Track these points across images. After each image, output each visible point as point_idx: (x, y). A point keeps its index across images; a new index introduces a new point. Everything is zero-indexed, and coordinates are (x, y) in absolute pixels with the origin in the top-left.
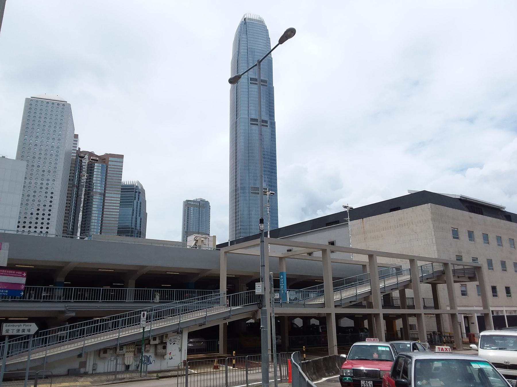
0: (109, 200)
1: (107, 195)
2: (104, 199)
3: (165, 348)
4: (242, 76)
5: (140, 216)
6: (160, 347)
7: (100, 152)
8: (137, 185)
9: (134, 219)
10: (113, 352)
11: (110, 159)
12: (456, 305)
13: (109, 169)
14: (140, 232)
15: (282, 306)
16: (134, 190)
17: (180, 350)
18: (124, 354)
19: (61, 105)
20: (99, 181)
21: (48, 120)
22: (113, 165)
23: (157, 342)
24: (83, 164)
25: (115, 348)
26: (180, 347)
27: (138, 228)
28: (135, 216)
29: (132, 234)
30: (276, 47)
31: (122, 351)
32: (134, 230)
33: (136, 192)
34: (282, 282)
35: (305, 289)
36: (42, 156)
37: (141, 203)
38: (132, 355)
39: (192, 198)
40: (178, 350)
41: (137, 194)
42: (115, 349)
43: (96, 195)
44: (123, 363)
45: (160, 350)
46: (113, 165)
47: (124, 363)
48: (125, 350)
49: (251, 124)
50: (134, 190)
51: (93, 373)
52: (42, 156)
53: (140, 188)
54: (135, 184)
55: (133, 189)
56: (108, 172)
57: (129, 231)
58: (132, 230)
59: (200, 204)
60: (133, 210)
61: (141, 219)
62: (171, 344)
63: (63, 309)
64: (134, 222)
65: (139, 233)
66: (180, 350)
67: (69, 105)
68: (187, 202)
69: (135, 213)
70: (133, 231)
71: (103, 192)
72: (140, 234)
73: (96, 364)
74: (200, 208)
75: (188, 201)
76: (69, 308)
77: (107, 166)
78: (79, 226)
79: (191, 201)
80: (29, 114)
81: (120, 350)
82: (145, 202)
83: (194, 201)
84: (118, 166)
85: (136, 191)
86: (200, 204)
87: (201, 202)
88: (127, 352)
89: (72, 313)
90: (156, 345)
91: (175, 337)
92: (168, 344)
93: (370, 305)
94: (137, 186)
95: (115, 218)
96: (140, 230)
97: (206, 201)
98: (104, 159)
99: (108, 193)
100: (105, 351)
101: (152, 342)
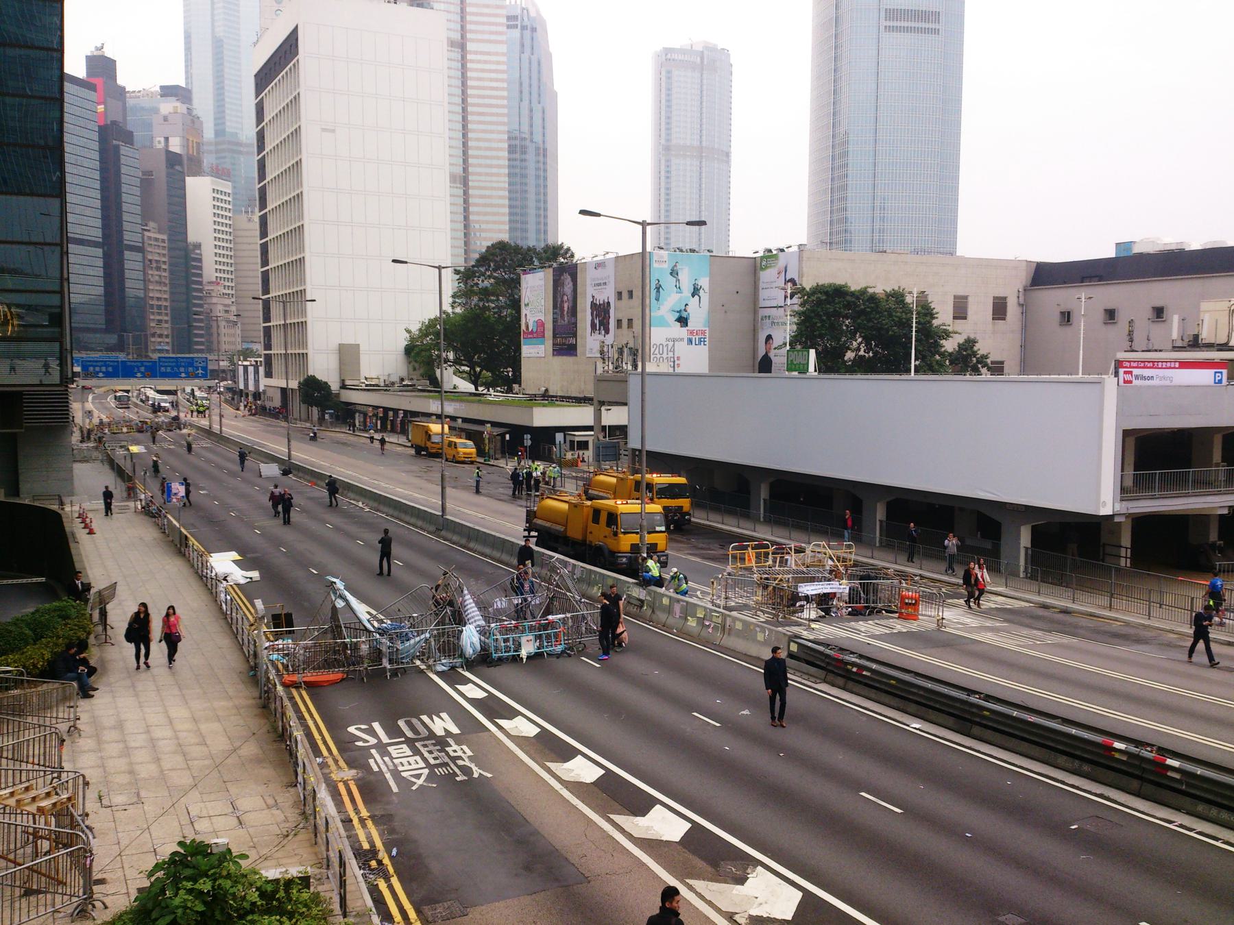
2: (463, 57)
8: (523, 6)
9: (525, 112)
14: (545, 150)
16: (519, 23)
27: (538, 138)
28: (528, 102)
29: (523, 157)
32: (528, 143)
33: (524, 28)
39: (678, 41)
41: (527, 33)
50: (519, 23)
53: (533, 14)
59: (702, 59)
60: (521, 84)
64: (525, 121)
65: (542, 151)
68: (666, 55)
71: (460, 38)
72: (545, 156)
74: (705, 72)
75: (667, 51)
82: (549, 56)
83: (682, 51)
85: (525, 24)
86: (702, 59)
87: (706, 53)
94: (523, 9)
95: (497, 115)
99: (472, 40)
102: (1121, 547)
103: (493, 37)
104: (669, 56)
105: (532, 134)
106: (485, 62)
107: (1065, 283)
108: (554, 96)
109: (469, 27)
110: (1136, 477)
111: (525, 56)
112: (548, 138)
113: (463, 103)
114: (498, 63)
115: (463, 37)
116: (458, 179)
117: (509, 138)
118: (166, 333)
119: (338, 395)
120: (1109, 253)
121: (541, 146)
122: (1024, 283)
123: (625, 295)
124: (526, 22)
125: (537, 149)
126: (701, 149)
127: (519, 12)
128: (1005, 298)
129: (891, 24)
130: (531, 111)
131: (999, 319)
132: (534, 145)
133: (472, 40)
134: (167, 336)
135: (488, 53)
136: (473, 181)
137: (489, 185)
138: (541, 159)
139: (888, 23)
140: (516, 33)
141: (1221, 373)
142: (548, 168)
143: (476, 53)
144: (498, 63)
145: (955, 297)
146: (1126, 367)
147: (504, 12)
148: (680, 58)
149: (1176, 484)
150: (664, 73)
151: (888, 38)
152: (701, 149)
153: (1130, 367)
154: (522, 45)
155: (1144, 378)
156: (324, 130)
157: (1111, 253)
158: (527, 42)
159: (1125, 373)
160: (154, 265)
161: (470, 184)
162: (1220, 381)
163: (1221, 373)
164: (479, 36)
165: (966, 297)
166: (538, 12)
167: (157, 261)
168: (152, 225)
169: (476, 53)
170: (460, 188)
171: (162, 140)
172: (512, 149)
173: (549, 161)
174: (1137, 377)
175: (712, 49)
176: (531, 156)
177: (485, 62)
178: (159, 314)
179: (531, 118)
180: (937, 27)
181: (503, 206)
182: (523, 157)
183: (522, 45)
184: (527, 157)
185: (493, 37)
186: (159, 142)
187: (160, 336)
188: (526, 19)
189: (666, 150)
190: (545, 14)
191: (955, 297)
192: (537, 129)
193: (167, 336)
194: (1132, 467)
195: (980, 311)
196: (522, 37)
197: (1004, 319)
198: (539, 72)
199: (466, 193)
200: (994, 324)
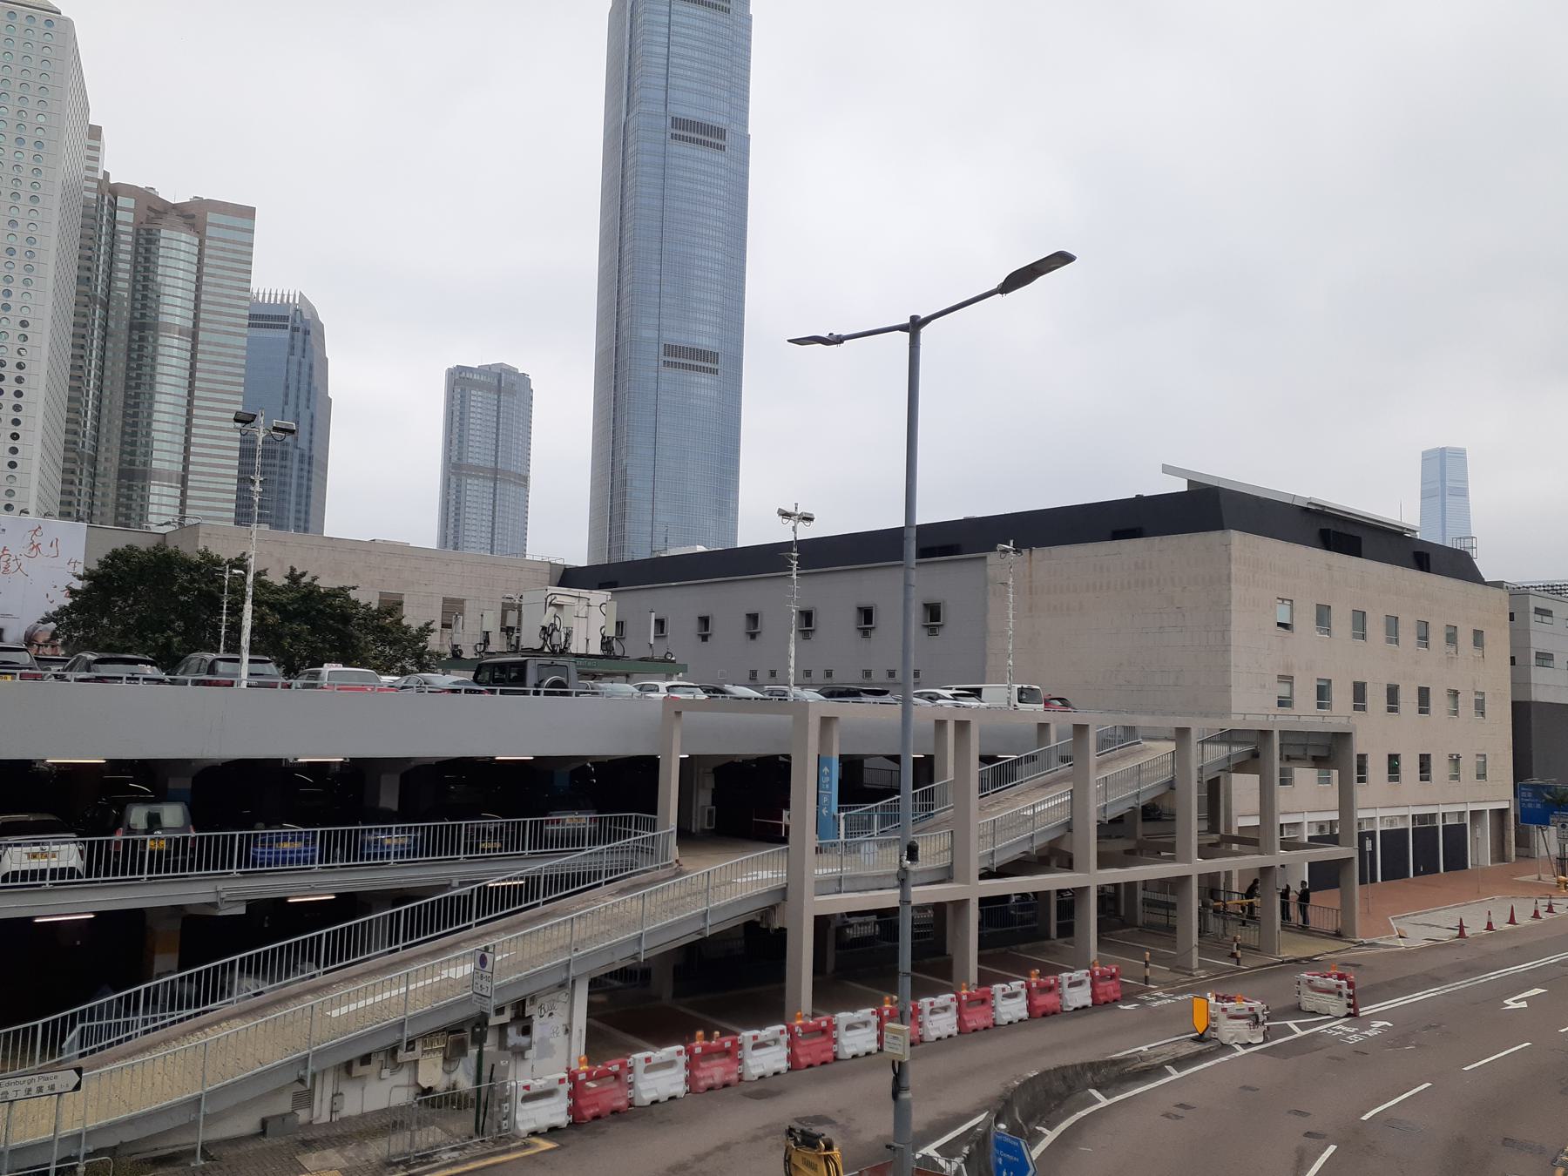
0: (212, 353)
1: (202, 336)
2: (194, 347)
3: (527, 1031)
4: (845, 342)
6: (512, 1032)
7: (174, 192)
10: (386, 1056)
12: (1276, 811)
14: (310, 458)
15: (843, 888)
17: (567, 1030)
18: (416, 1062)
19: (40, 22)
22: (219, 239)
23: (506, 1018)
25: (393, 1051)
26: (565, 1020)
29: (284, 463)
30: (985, 298)
31: (410, 1053)
32: (290, 449)
33: (295, 329)
34: (827, 786)
35: (891, 802)
37: (311, 368)
38: (439, 1058)
40: (561, 1031)
41: (299, 335)
42: (393, 1051)
43: (168, 334)
44: (412, 1082)
45: (513, 1037)
46: (219, 239)
47: (418, 1084)
48: (419, 1047)
49: (672, 138)
50: (289, 324)
51: (333, 1120)
53: (307, 316)
54: (291, 301)
55: (286, 318)
57: (275, 451)
58: (285, 449)
61: (312, 417)
62: (541, 1017)
65: (306, 459)
66: (568, 1031)
67: (68, 23)
68: (461, 373)
72: (310, 464)
73: (341, 1094)
75: (461, 369)
76: (229, 896)
78: (243, 643)
79: (471, 370)
80: (16, 186)
81: (407, 1050)
84: (234, 242)
85: (296, 325)
86: (499, 381)
88: (424, 1052)
89: (237, 906)
90: (502, 1028)
91: (554, 996)
92: (536, 1019)
93: (1068, 864)
96: (310, 449)
97: (520, 372)
98: (192, 216)
99: (205, 330)
100: (366, 1059)
101: (494, 1020)
103: (232, 329)
106: (220, 354)
109: (202, 315)
111: (295, 359)
112: (315, 446)
113: (189, 395)
114: (235, 356)
115: (195, 325)
116: (174, 476)
121: (306, 453)
125: (302, 456)
126: (496, 471)
132: (298, 451)
133: (205, 330)
135: (224, 346)
136: (192, 481)
137: (212, 486)
138: (306, 467)
139: (667, 359)
140: (285, 335)
142: (314, 477)
143: (209, 343)
144: (235, 356)
145: (445, 600)
147: (247, 304)
148: (475, 377)
151: (668, 373)
152: (496, 471)
154: (293, 347)
158: (299, 344)
161: (190, 483)
164: (215, 327)
165: (462, 601)
169: (209, 343)
170: (177, 488)
175: (511, 372)
177: (220, 354)
180: (716, 368)
181: (229, 510)
182: (284, 463)
183: (293, 347)
184: (289, 464)
185: (232, 329)
188: (298, 320)
189: (456, 469)
191: (445, 600)
196: (292, 338)
198: (310, 376)
199: (183, 493)
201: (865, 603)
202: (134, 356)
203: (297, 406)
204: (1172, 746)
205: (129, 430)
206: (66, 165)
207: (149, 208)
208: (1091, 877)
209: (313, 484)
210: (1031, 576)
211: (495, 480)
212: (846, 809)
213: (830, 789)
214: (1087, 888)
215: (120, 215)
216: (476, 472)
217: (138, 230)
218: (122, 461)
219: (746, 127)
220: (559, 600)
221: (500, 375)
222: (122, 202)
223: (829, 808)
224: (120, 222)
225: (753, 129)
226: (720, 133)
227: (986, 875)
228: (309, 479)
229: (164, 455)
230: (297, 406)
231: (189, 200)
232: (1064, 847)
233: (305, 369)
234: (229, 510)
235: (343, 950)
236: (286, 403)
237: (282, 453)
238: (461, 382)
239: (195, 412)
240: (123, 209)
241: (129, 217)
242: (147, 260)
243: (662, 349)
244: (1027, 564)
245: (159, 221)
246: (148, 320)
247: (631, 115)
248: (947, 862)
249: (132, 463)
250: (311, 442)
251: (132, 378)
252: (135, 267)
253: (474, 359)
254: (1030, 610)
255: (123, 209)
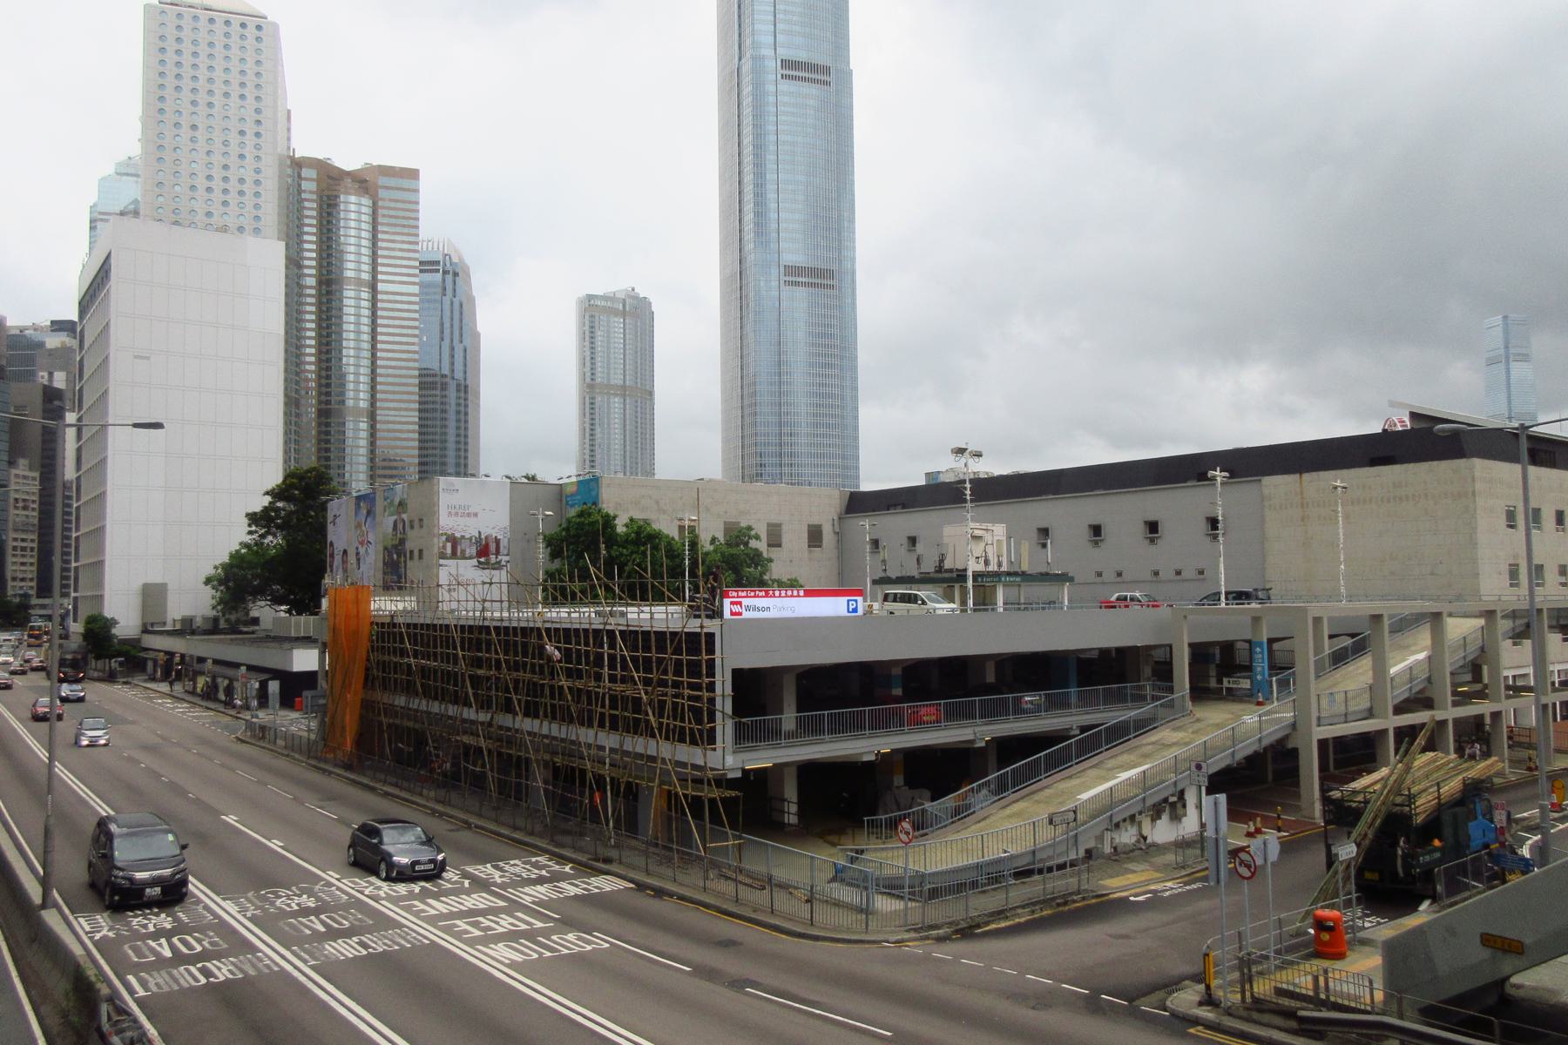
1: (380, 286)
5: (461, 342)
7: (347, 161)
11: (382, 181)
13: (380, 212)
14: (466, 387)
19: (251, 29)
20: (353, 247)
21: (219, 74)
22: (391, 200)
24: (304, 196)
27: (459, 375)
32: (448, 380)
36: (217, 184)
38: (1149, 819)
41: (449, 278)
46: (391, 200)
52: (217, 184)
53: (455, 260)
54: (441, 249)
55: (437, 263)
56: (380, 220)
57: (436, 383)
58: (445, 380)
59: (624, 306)
60: (442, 324)
61: (465, 350)
63: (971, 737)
65: (463, 388)
69: (447, 332)
70: (446, 384)
72: (466, 392)
75: (590, 297)
77: (375, 204)
79: (596, 297)
82: (472, 300)
83: (604, 298)
86: (624, 306)
96: (465, 379)
98: (364, 182)
102: (785, 800)
104: (592, 302)
105: (453, 371)
107: (874, 511)
108: (476, 336)
110: (799, 720)
117: (420, 376)
118: (30, 576)
119: (139, 640)
120: (920, 481)
122: (839, 510)
123: (416, 524)
124: (448, 267)
125: (458, 385)
127: (440, 258)
128: (820, 526)
129: (791, 279)
130: (452, 349)
131: (815, 546)
134: (31, 580)
137: (398, 419)
138: (462, 395)
139: (787, 279)
140: (439, 276)
141: (856, 601)
143: (387, 293)
146: (733, 597)
147: (416, 255)
149: (841, 727)
150: (587, 317)
152: (624, 387)
153: (738, 597)
155: (756, 609)
156: (136, 357)
157: (922, 482)
159: (732, 603)
160: (20, 504)
161: (378, 418)
162: (855, 610)
163: (856, 601)
165: (779, 525)
166: (461, 259)
167: (24, 500)
168: (22, 462)
171: (45, 374)
172: (422, 386)
173: (470, 397)
174: (748, 608)
176: (452, 393)
178: (23, 556)
179: (453, 356)
181: (413, 440)
183: (445, 289)
186: (43, 377)
187: (23, 580)
188: (448, 264)
189: (592, 391)
190: (468, 261)
191: (769, 525)
192: (459, 366)
193: (31, 580)
194: (794, 707)
195: (795, 538)
196: (444, 280)
197: (820, 546)
200: (810, 552)
201: (1151, 518)
202: (324, 309)
203: (452, 340)
204: (1482, 622)
205: (324, 373)
206: (281, 149)
207: (330, 177)
208: (1450, 713)
209: (470, 411)
210: (1302, 493)
211: (624, 396)
212: (1277, 674)
213: (1263, 662)
214: (1447, 720)
215: (305, 185)
216: (609, 389)
217: (321, 197)
218: (320, 402)
219: (848, 63)
220: (977, 533)
221: (624, 300)
222: (306, 172)
223: (1263, 675)
224: (304, 191)
225: (854, 64)
226: (826, 70)
227: (1399, 709)
228: (466, 406)
229: (356, 394)
230: (452, 340)
231: (359, 167)
232: (1428, 694)
233: (456, 306)
234: (413, 440)
235: (1058, 763)
236: (442, 339)
237: (442, 384)
238: (594, 312)
239: (379, 354)
240: (306, 179)
241: (312, 186)
242: (329, 222)
243: (782, 269)
244: (1298, 485)
245: (338, 188)
246: (333, 276)
247: (743, 61)
248: (1368, 705)
249: (328, 402)
250: (465, 372)
251: (323, 328)
252: (321, 230)
253: (603, 285)
254: (1303, 520)
255: (306, 179)
